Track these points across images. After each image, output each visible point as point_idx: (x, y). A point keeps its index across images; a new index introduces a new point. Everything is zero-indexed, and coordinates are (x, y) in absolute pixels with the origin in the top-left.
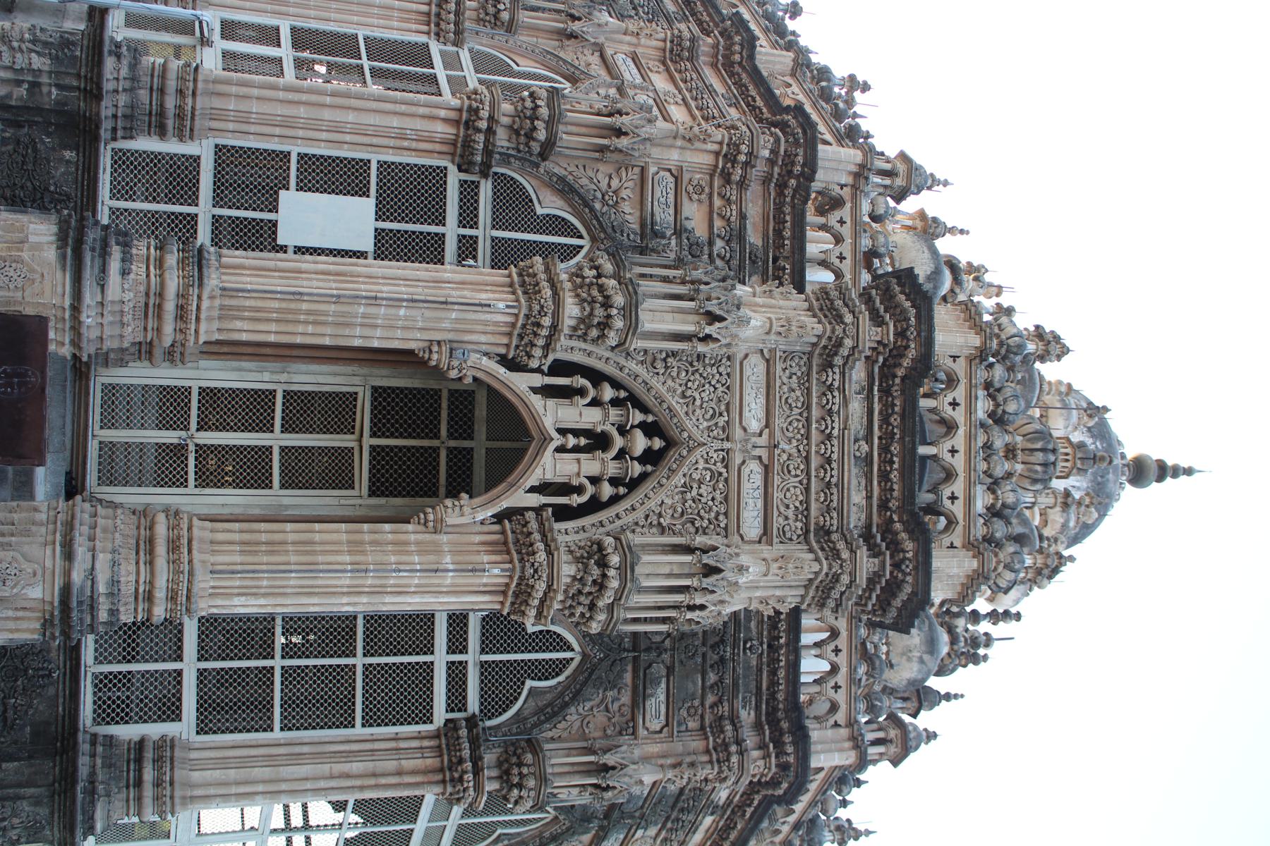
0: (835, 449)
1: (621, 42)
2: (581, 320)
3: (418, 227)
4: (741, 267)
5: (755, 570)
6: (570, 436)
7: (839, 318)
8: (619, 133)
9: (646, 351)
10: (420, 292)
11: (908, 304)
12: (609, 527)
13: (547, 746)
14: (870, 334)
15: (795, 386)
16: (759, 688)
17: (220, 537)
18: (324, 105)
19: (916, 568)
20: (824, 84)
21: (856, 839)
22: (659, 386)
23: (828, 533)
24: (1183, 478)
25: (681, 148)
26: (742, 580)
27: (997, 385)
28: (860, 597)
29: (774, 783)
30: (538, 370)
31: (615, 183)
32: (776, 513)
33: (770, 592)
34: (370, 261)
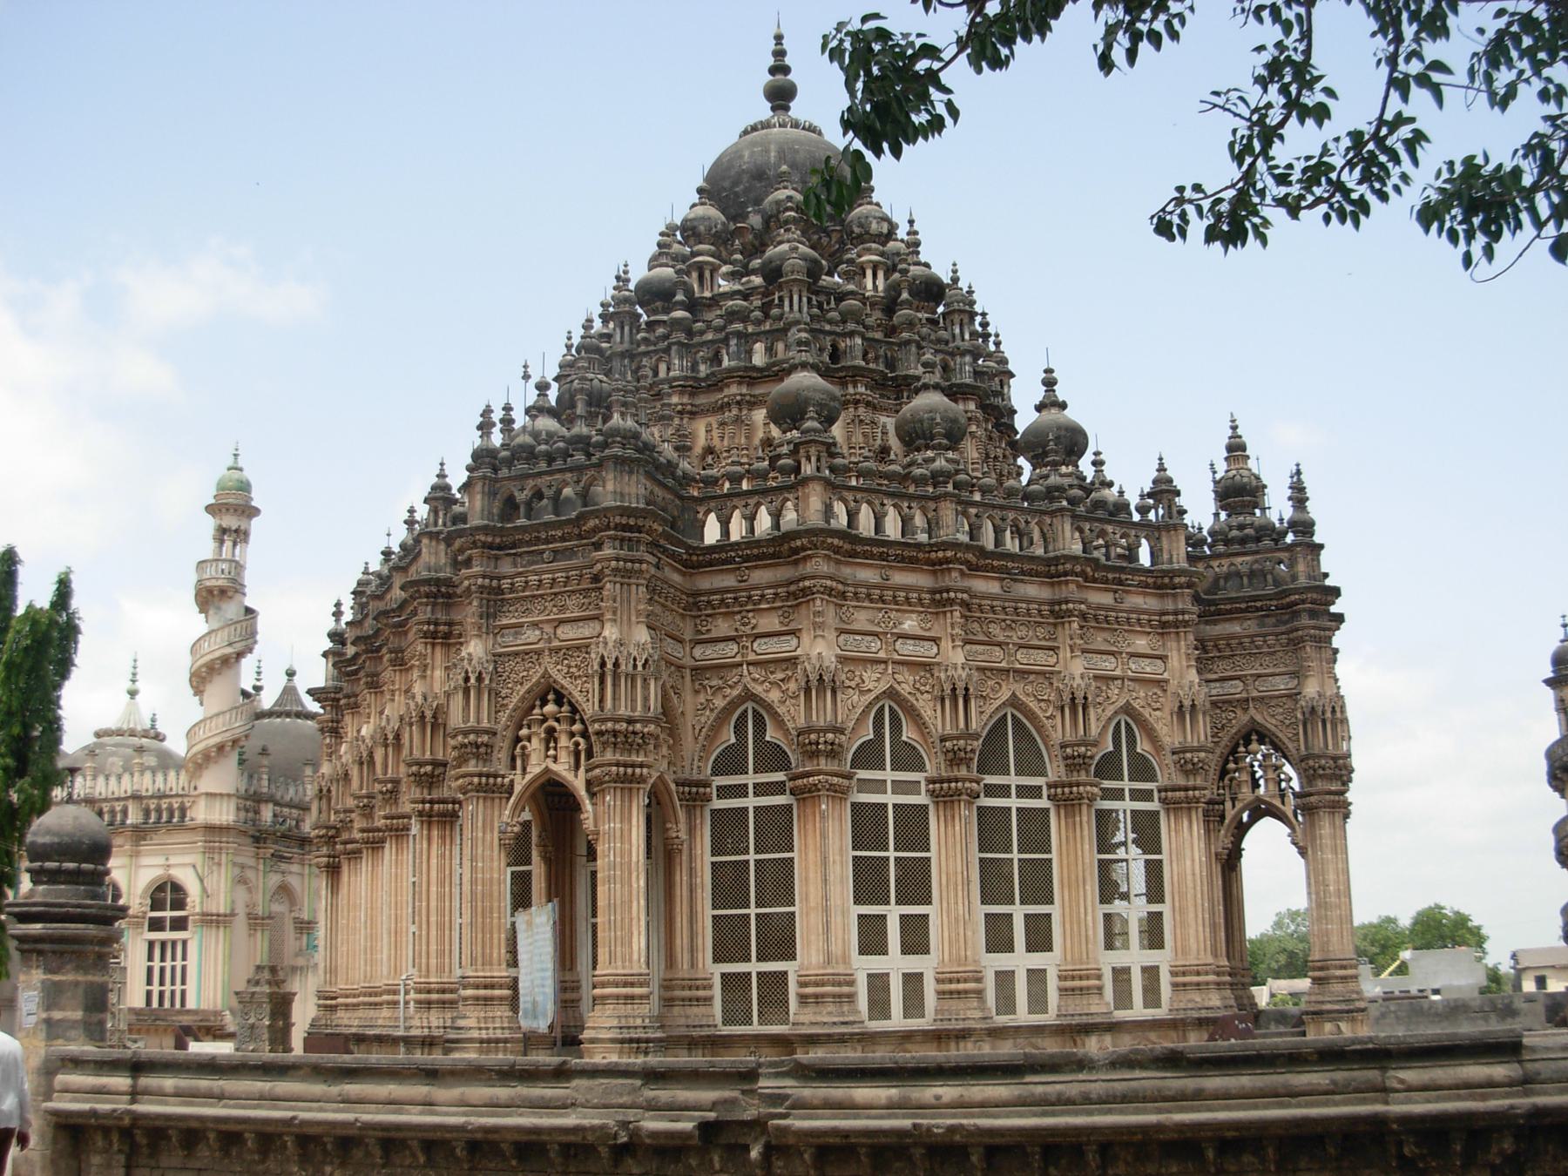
8: (423, 717)
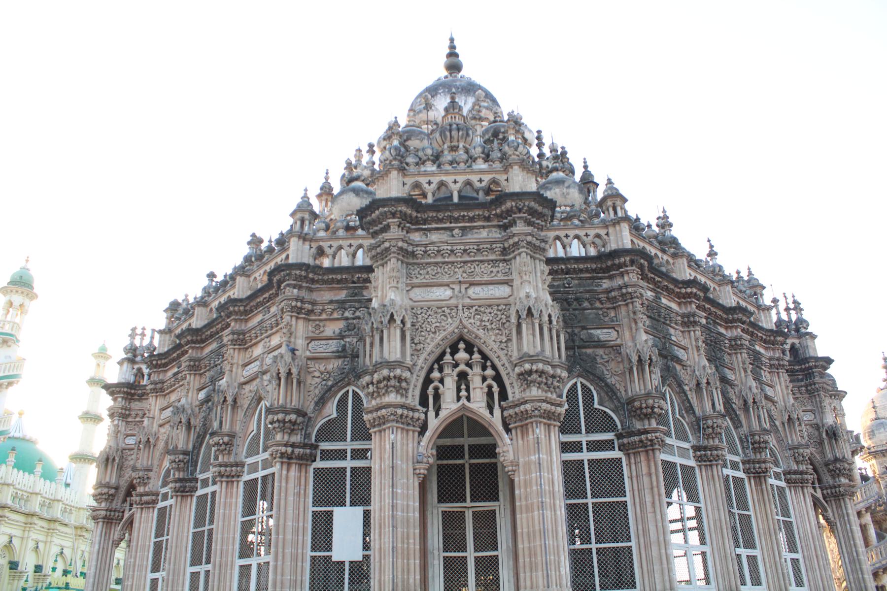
0: (459, 247)
1: (236, 373)
2: (397, 392)
3: (348, 483)
4: (359, 301)
5: (528, 289)
6: (461, 394)
7: (387, 250)
8: (289, 373)
9: (412, 355)
10: (387, 481)
11: (377, 212)
12: (509, 369)
13: (630, 394)
14: (395, 232)
15: (425, 271)
16: (590, 278)
17: (528, 583)
18: (284, 539)
19: (521, 200)
20: (253, 259)
21: (668, 218)
22: (430, 346)
23: (504, 249)
24: (456, 43)
25: (295, 338)
26: (534, 295)
27: (417, 160)
28: (538, 229)
29: (641, 267)
30: (426, 414)
31: (317, 374)
32: (496, 278)
33: (539, 279)
34: (371, 508)
